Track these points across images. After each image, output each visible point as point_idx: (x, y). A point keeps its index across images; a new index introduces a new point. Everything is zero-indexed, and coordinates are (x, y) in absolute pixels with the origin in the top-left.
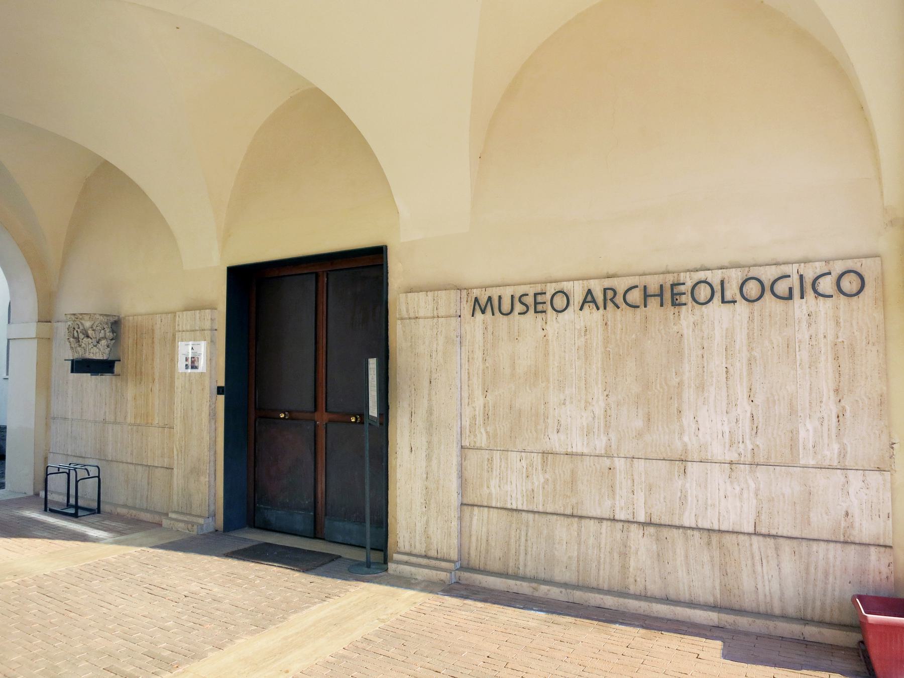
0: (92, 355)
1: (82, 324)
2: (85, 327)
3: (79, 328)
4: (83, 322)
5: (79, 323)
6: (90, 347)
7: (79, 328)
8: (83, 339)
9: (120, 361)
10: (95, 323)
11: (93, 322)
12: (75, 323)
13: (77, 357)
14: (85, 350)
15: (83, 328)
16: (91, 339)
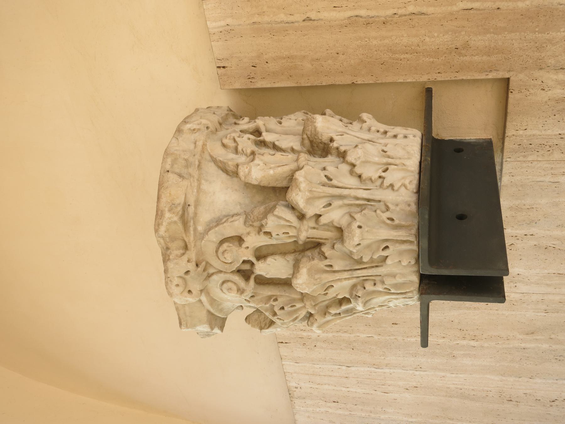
0: (392, 177)
1: (218, 222)
2: (238, 209)
3: (240, 240)
4: (205, 217)
5: (213, 237)
6: (353, 181)
7: (240, 240)
8: (302, 217)
9: (429, 92)
10: (214, 160)
11: (211, 168)
12: (216, 264)
13: (408, 261)
14: (362, 208)
15: (242, 219)
16: (299, 169)
